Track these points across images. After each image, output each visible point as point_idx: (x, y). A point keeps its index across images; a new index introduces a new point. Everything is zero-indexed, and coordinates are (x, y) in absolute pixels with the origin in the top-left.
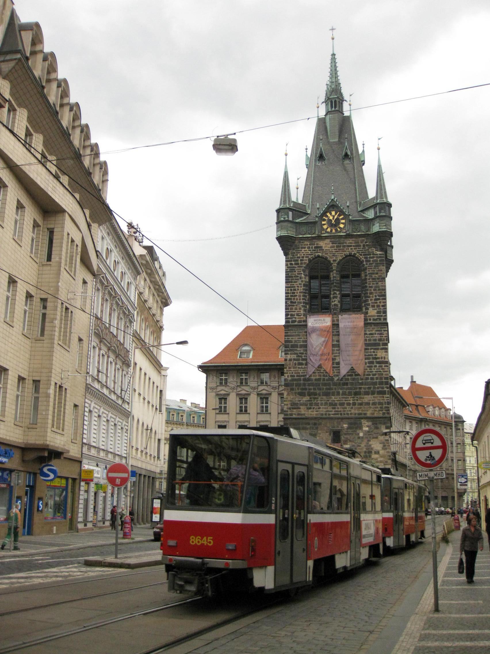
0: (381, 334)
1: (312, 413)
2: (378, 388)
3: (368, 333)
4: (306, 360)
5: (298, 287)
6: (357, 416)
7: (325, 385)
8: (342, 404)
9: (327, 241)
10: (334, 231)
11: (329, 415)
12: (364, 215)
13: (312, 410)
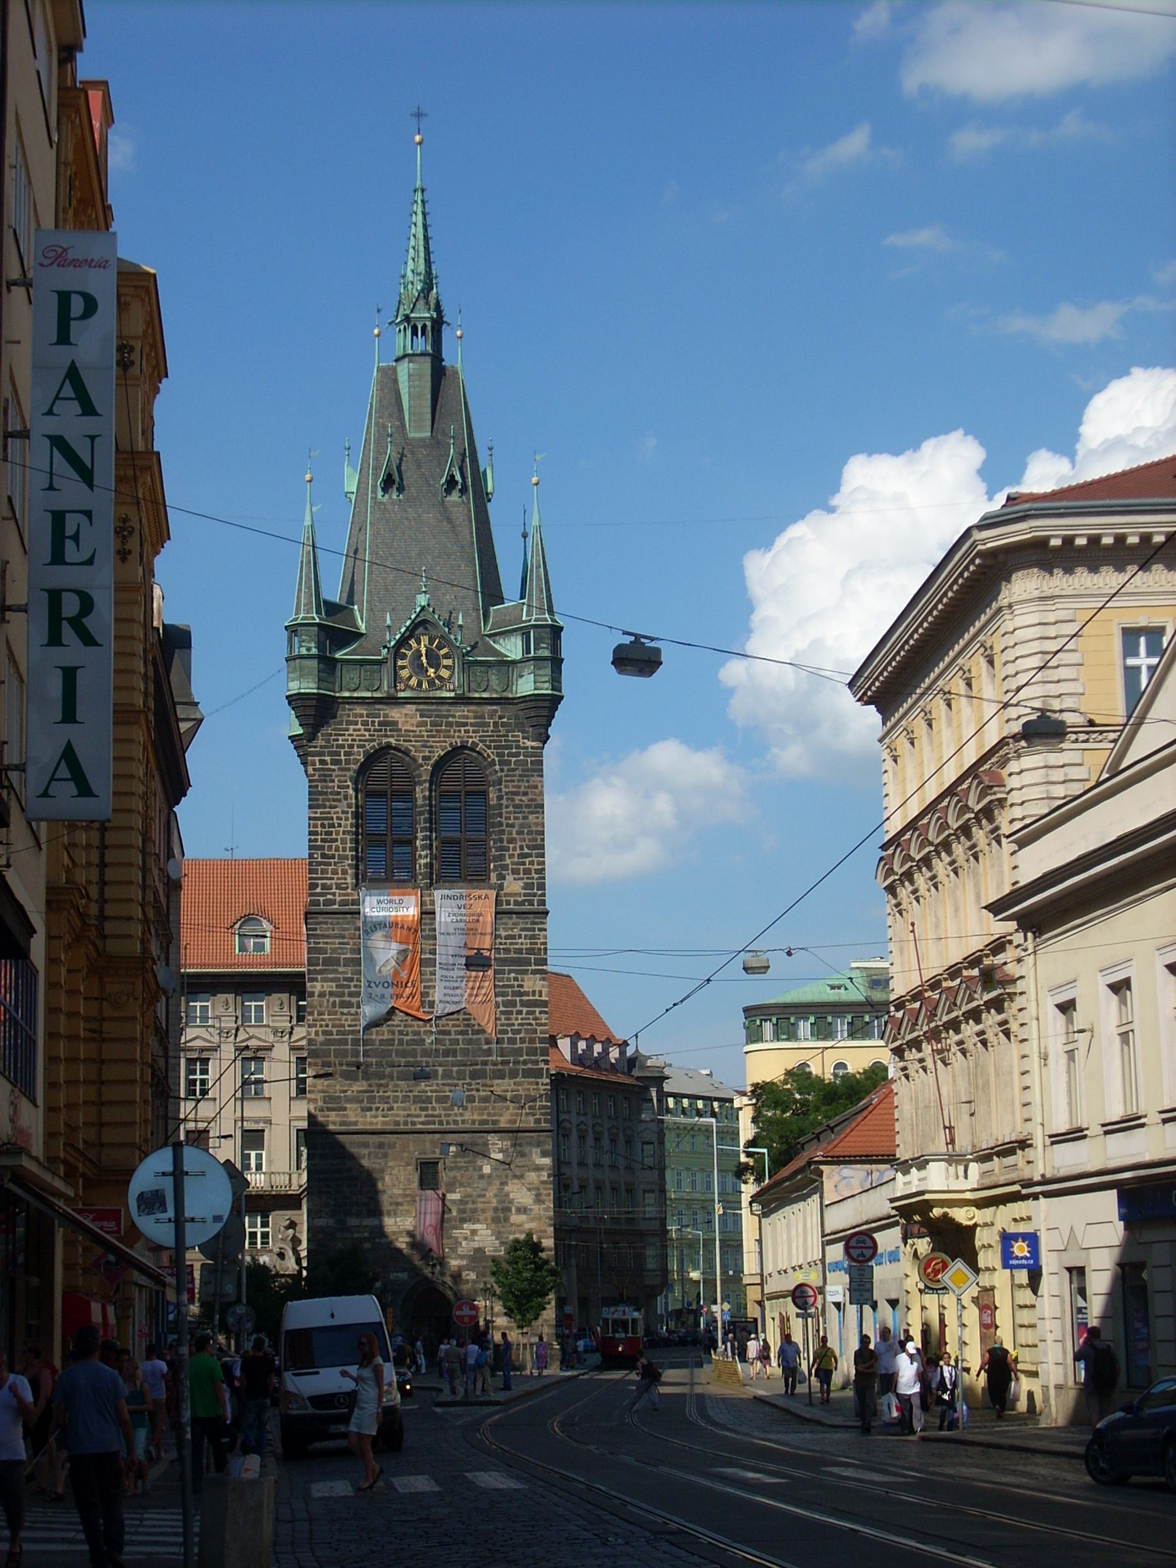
0: (533, 937)
1: (374, 1120)
2: (525, 1062)
3: (504, 934)
4: (358, 994)
5: (339, 818)
6: (477, 1126)
7: (404, 1054)
8: (441, 1100)
9: (410, 709)
10: (425, 685)
11: (414, 1123)
12: (496, 646)
13: (373, 1112)
